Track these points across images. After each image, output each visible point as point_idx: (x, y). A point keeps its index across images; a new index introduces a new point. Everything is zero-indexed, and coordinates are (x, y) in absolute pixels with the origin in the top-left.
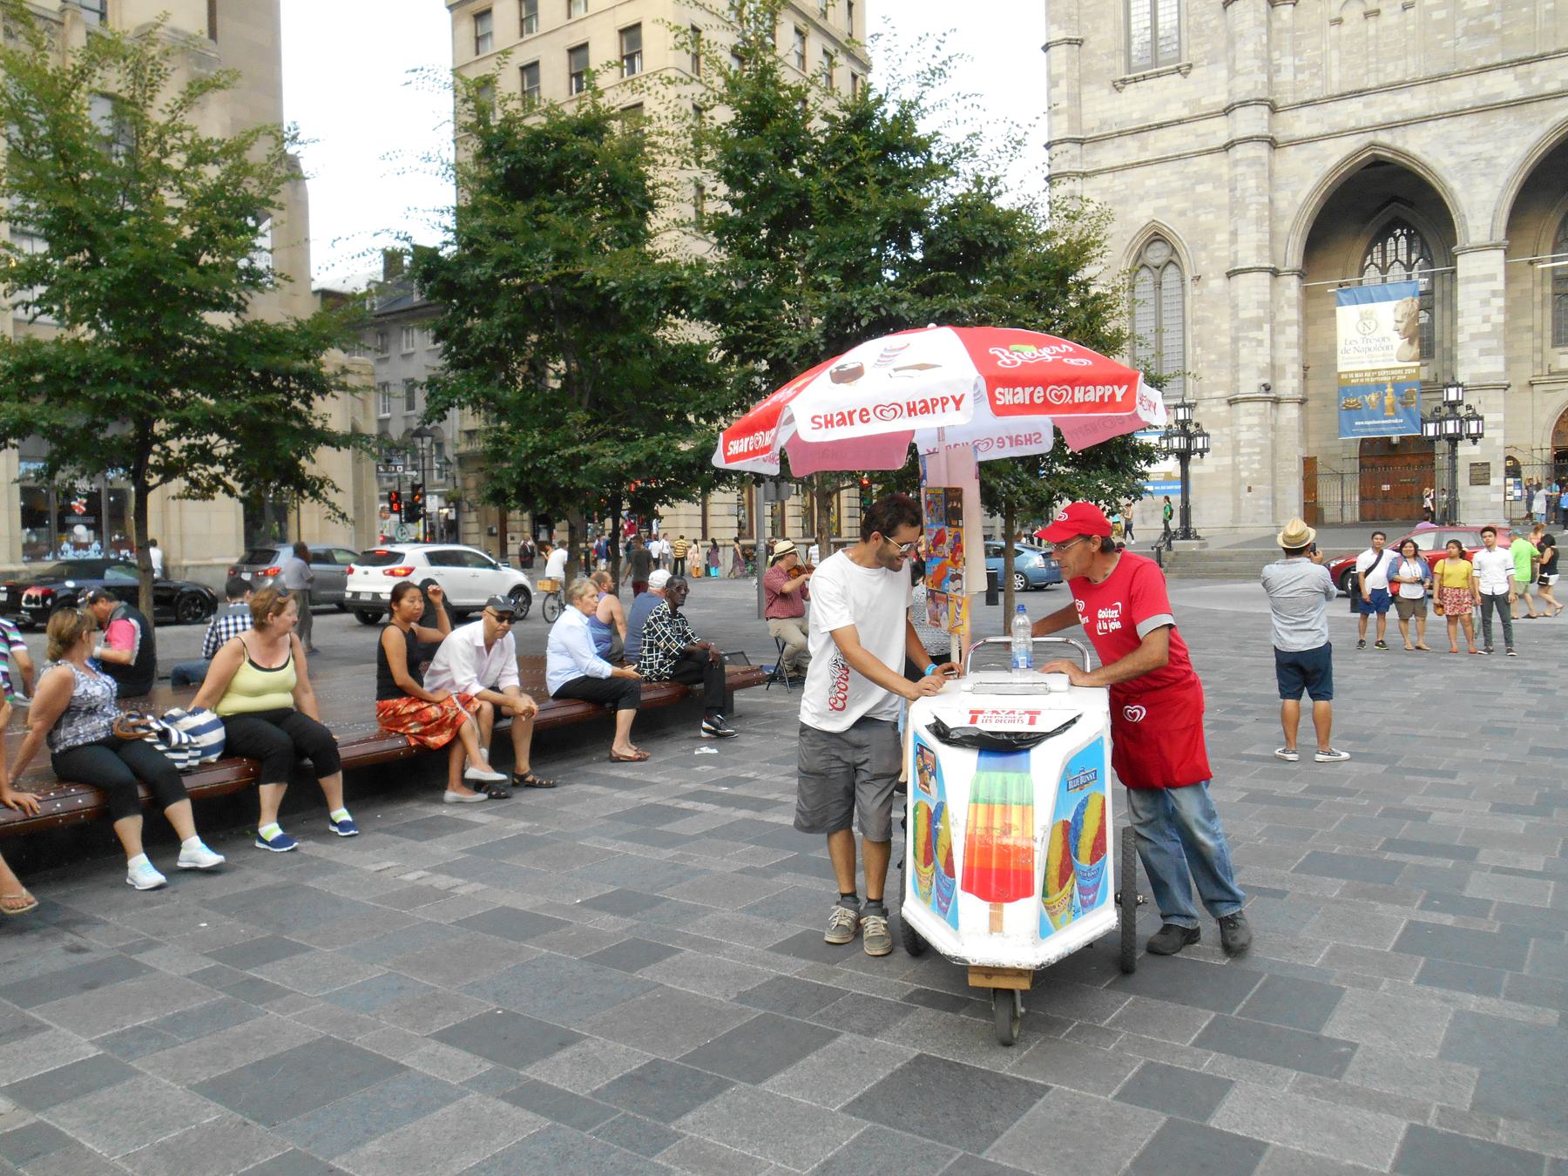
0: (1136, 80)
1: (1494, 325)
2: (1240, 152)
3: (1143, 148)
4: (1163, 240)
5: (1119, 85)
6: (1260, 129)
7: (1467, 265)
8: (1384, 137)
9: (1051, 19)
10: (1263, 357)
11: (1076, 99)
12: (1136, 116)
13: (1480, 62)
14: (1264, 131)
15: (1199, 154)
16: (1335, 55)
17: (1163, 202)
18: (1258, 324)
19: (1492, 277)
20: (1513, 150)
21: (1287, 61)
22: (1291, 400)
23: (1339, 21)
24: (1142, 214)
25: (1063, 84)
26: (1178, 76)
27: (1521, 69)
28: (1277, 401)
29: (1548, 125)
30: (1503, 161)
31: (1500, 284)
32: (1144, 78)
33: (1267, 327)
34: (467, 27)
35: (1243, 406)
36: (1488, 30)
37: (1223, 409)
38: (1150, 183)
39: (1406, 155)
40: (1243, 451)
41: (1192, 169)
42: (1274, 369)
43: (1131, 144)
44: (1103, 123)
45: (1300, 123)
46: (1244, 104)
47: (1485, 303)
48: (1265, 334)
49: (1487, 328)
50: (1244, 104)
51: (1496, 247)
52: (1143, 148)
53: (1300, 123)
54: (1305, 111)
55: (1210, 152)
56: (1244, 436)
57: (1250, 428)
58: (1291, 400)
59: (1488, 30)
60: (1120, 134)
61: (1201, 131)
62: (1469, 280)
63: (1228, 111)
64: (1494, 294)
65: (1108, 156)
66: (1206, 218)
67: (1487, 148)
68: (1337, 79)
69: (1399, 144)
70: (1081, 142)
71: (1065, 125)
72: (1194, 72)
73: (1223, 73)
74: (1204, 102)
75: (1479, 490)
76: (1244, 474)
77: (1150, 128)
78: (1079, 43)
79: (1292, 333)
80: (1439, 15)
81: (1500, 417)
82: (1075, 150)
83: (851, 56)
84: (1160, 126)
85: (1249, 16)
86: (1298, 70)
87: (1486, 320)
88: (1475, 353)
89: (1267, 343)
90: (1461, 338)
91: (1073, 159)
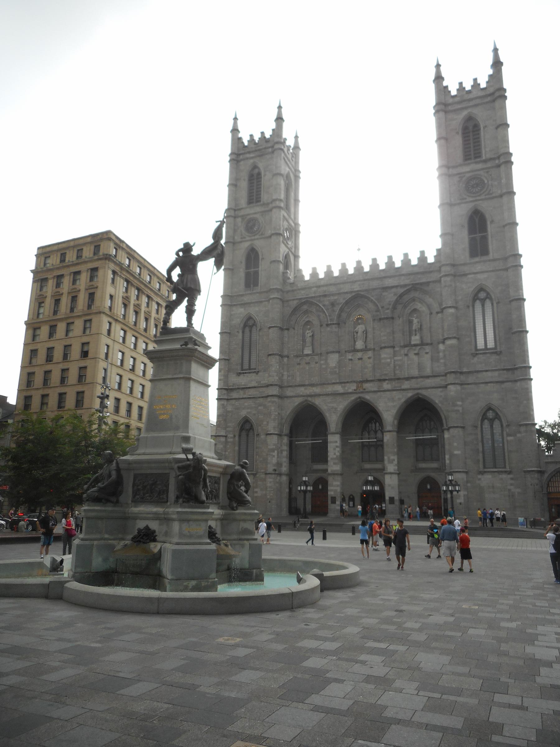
0: (243, 373)
1: (337, 456)
2: (269, 399)
3: (244, 394)
4: (249, 422)
5: (239, 374)
7: (330, 438)
8: (310, 399)
10: (274, 461)
12: (243, 384)
13: (333, 381)
15: (259, 397)
16: (298, 373)
17: (249, 410)
18: (273, 450)
19: (336, 442)
20: (341, 407)
21: (285, 373)
22: (284, 474)
23: (299, 364)
24: (243, 413)
25: (223, 371)
26: (255, 374)
27: (343, 385)
28: (280, 474)
29: (349, 401)
30: (339, 409)
31: (338, 444)
32: (246, 373)
33: (276, 452)
34: (31, 332)
35: (268, 476)
37: (263, 476)
38: (246, 404)
39: (315, 404)
40: (268, 489)
41: (258, 402)
42: (279, 464)
43: (241, 392)
44: (234, 385)
45: (289, 392)
46: (271, 385)
47: (335, 449)
48: (275, 453)
49: (335, 456)
50: (271, 385)
51: (337, 433)
52: (244, 394)
53: (289, 392)
54: (289, 388)
55: (262, 397)
56: (269, 485)
57: (270, 482)
58: (284, 474)
60: (238, 388)
61: (261, 391)
62: (331, 442)
63: (267, 386)
64: (337, 447)
65: (235, 395)
66: (261, 417)
67: (335, 405)
69: (313, 401)
71: (222, 384)
72: (260, 373)
73: (267, 375)
74: (262, 382)
75: (333, 505)
76: (268, 497)
77: (247, 388)
79: (285, 453)
80: (324, 366)
81: (338, 483)
82: (225, 392)
84: (249, 388)
86: (288, 376)
87: (335, 454)
88: (332, 463)
89: (276, 457)
90: (329, 459)
91: (224, 394)
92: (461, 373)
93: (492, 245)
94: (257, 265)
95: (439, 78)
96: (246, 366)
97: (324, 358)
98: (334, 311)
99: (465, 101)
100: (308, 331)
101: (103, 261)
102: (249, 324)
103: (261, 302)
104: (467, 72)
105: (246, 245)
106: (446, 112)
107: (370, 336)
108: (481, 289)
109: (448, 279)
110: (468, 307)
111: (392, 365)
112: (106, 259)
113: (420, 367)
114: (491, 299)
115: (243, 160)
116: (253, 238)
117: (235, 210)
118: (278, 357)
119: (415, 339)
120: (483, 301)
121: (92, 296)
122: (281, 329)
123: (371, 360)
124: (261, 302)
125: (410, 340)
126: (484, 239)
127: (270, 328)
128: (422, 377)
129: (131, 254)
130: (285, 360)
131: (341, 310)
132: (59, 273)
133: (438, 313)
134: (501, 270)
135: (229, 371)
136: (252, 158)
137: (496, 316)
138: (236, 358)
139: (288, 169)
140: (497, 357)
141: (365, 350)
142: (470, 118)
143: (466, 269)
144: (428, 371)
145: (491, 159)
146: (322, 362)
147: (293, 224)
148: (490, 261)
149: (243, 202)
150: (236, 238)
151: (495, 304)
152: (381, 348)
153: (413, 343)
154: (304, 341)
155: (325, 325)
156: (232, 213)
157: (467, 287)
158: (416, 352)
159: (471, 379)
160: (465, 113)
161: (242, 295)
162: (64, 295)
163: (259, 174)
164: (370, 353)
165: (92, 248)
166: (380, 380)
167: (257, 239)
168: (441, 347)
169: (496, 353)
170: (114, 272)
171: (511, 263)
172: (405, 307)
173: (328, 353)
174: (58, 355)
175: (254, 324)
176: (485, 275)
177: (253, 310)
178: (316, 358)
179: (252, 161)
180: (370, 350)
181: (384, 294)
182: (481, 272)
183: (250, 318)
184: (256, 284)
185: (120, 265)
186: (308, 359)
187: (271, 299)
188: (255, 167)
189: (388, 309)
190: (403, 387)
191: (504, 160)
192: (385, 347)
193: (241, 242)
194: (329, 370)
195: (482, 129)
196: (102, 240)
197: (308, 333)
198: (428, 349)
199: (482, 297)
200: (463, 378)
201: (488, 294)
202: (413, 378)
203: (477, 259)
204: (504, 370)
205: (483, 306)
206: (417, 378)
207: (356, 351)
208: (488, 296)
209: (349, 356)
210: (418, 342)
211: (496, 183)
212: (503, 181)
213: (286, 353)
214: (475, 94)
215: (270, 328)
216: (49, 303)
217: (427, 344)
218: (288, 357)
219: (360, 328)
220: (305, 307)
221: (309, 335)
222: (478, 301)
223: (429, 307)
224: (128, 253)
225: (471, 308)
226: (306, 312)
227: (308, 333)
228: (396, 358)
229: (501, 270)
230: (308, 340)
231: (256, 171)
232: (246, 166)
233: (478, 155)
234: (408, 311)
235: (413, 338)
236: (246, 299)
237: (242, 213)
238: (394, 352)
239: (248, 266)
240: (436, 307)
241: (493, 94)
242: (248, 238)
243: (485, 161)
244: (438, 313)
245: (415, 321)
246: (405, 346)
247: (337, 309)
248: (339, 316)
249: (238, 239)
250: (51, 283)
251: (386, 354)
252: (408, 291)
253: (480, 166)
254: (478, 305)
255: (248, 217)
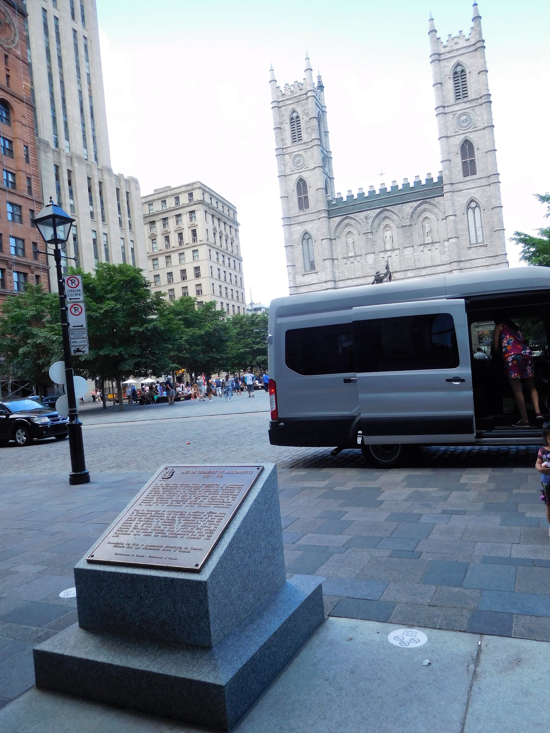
5: (304, 275)
6: (332, 286)
9: (288, 260)
11: (294, 278)
14: (333, 287)
21: (337, 271)
25: (291, 274)
36: (373, 268)
43: (307, 287)
44: (301, 283)
52: (309, 288)
59: (373, 268)
68: (347, 275)
70: (296, 287)
78: (294, 266)
82: (295, 289)
83: (238, 259)
85: (328, 263)
86: (339, 273)
92: (461, 261)
93: (479, 166)
94: (306, 192)
95: (433, 31)
96: (308, 268)
97: (363, 258)
98: (367, 223)
99: (453, 50)
100: (349, 239)
101: (198, 205)
102: (306, 237)
103: (313, 220)
104: (455, 24)
105: (296, 177)
106: (440, 60)
107: (395, 239)
108: (472, 201)
109: (449, 194)
110: (464, 214)
111: (413, 259)
112: (200, 203)
113: (432, 259)
114: (479, 207)
115: (284, 106)
116: (300, 171)
117: (283, 149)
118: (331, 260)
119: (428, 240)
120: (474, 209)
121: (194, 233)
122: (331, 239)
123: (398, 257)
124: (313, 220)
125: (424, 240)
126: (473, 162)
127: (322, 240)
128: (433, 266)
129: (213, 195)
130: (336, 261)
131: (373, 222)
132: (164, 216)
133: (442, 219)
134: (485, 186)
135: (295, 274)
136: (291, 104)
137: (483, 219)
138: (300, 264)
139: (318, 109)
140: (485, 248)
141: (393, 250)
142: (458, 65)
143: (461, 186)
144: (438, 262)
145: (476, 99)
146: (362, 261)
147: (326, 153)
148: (477, 179)
149: (289, 142)
150: (286, 171)
151: (482, 211)
152: (404, 248)
153: (426, 242)
154: (347, 246)
155: (362, 234)
156: (280, 151)
157: (462, 199)
158: (429, 248)
159: (468, 265)
160: (454, 61)
161: (298, 216)
162: (171, 232)
163: (298, 117)
164: (397, 252)
165: (187, 195)
166: (405, 271)
167: (304, 171)
168: (446, 243)
169: (484, 246)
170: (206, 212)
171: (493, 179)
172: (419, 216)
173: (366, 254)
174: (177, 276)
175: (310, 238)
176: (475, 190)
177: (308, 227)
178: (358, 258)
179: (291, 107)
180: (396, 249)
181: (404, 207)
182: (471, 189)
183: (306, 233)
184: (307, 206)
185: (208, 205)
186: (352, 259)
187: (321, 218)
188: (294, 111)
189: (407, 219)
190: (421, 274)
191: (486, 100)
192: (406, 247)
193: (292, 174)
194: (368, 266)
195: (468, 74)
196: (193, 189)
197: (350, 241)
198: (437, 245)
199: (473, 206)
200: (462, 265)
201: (477, 203)
202: (429, 267)
203: (468, 178)
204: (489, 257)
205: (474, 212)
206: (430, 267)
207: (386, 251)
208: (478, 206)
209: (382, 255)
210: (430, 241)
211: (480, 118)
212: (485, 117)
213: (335, 257)
214: (462, 43)
215: (322, 240)
216: (160, 240)
217: (436, 242)
218: (337, 259)
219: (388, 234)
220: (346, 221)
221: (351, 242)
222: (470, 209)
223: (436, 215)
224: (210, 194)
225: (466, 215)
226: (348, 225)
227: (350, 241)
228: (415, 254)
229: (485, 186)
230: (351, 245)
231: (295, 115)
232: (286, 112)
233: (465, 95)
234: (421, 219)
235: (426, 238)
236: (302, 219)
237: (289, 150)
238: (414, 249)
239: (299, 193)
240: (441, 216)
241: (475, 44)
242: (297, 171)
243: (471, 101)
244: (442, 219)
245: (427, 226)
246: (421, 245)
247: (370, 221)
248: (372, 226)
249: (288, 172)
250: (159, 225)
251: (408, 252)
252: (421, 204)
253: (468, 105)
254: (470, 211)
255: (294, 154)
